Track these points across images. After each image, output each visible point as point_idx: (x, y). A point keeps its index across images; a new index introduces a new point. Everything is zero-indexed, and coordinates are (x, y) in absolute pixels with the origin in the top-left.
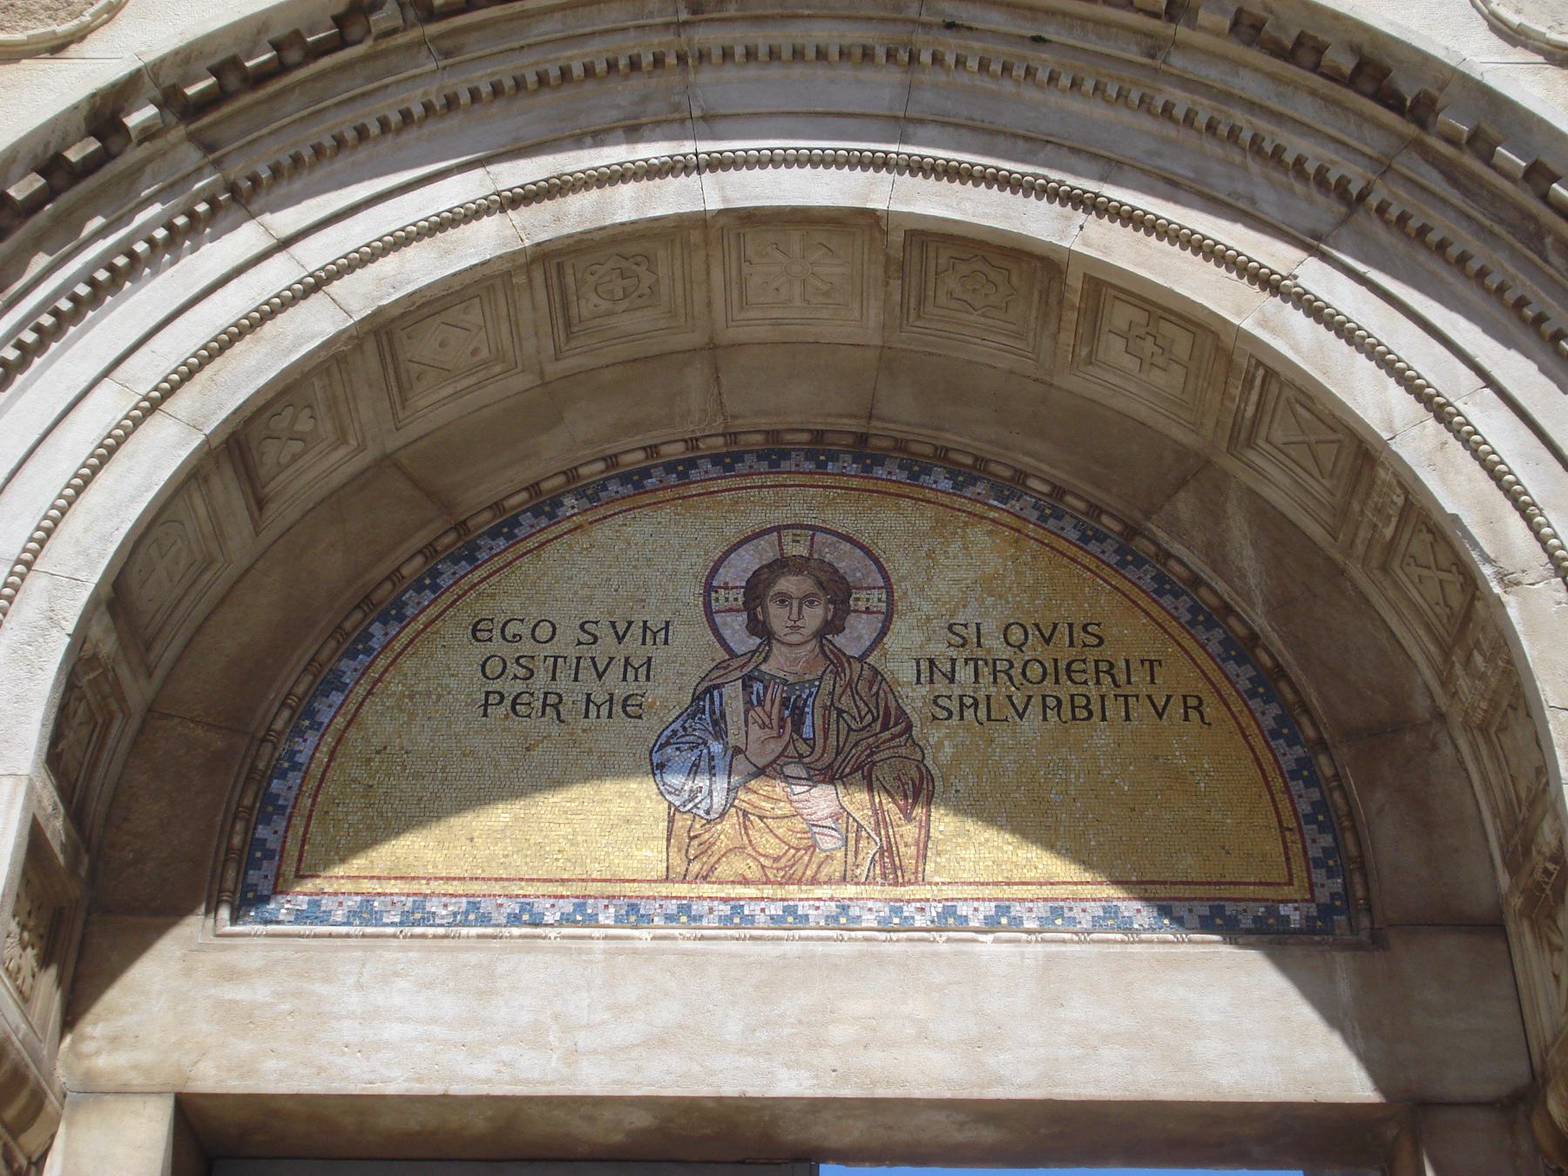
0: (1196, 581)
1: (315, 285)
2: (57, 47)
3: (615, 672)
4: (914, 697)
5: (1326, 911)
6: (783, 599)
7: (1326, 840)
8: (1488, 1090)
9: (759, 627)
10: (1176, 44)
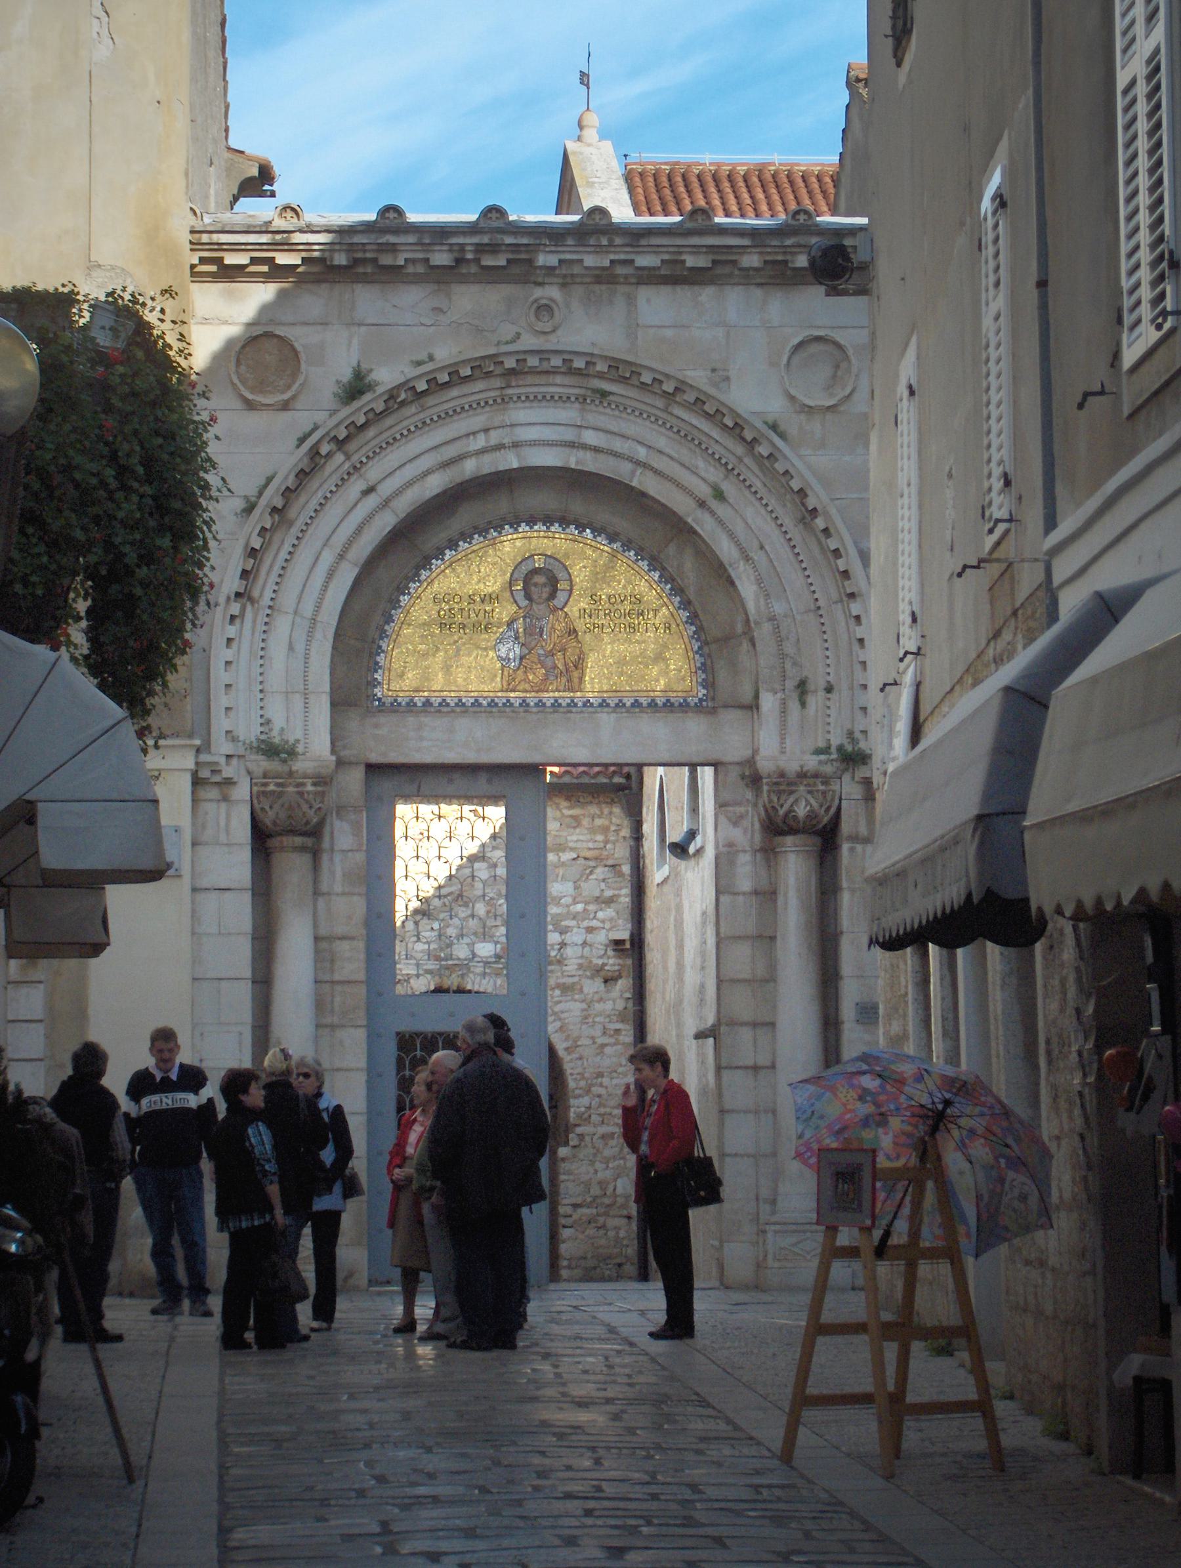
0: (673, 580)
1: (386, 503)
2: (285, 406)
3: (482, 614)
4: (580, 625)
5: (701, 700)
6: (536, 585)
7: (703, 676)
8: (736, 759)
9: (528, 596)
10: (676, 402)
